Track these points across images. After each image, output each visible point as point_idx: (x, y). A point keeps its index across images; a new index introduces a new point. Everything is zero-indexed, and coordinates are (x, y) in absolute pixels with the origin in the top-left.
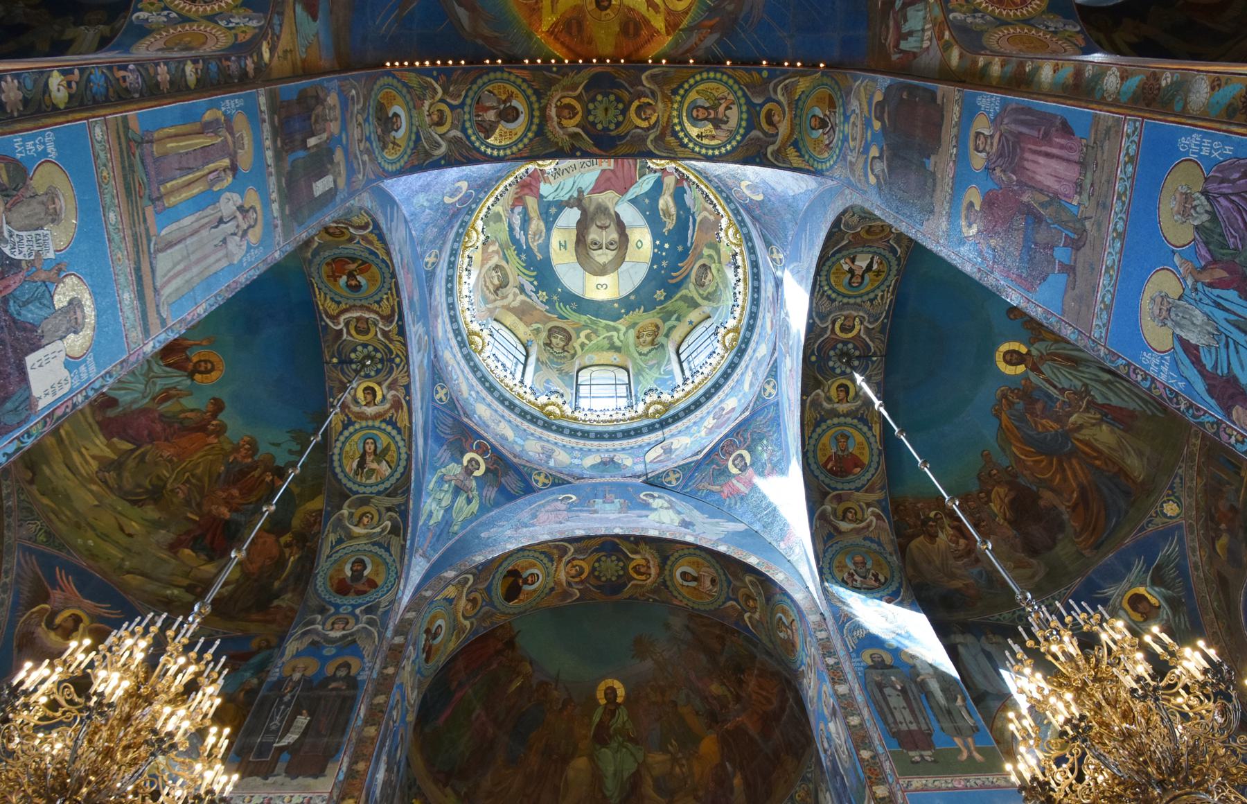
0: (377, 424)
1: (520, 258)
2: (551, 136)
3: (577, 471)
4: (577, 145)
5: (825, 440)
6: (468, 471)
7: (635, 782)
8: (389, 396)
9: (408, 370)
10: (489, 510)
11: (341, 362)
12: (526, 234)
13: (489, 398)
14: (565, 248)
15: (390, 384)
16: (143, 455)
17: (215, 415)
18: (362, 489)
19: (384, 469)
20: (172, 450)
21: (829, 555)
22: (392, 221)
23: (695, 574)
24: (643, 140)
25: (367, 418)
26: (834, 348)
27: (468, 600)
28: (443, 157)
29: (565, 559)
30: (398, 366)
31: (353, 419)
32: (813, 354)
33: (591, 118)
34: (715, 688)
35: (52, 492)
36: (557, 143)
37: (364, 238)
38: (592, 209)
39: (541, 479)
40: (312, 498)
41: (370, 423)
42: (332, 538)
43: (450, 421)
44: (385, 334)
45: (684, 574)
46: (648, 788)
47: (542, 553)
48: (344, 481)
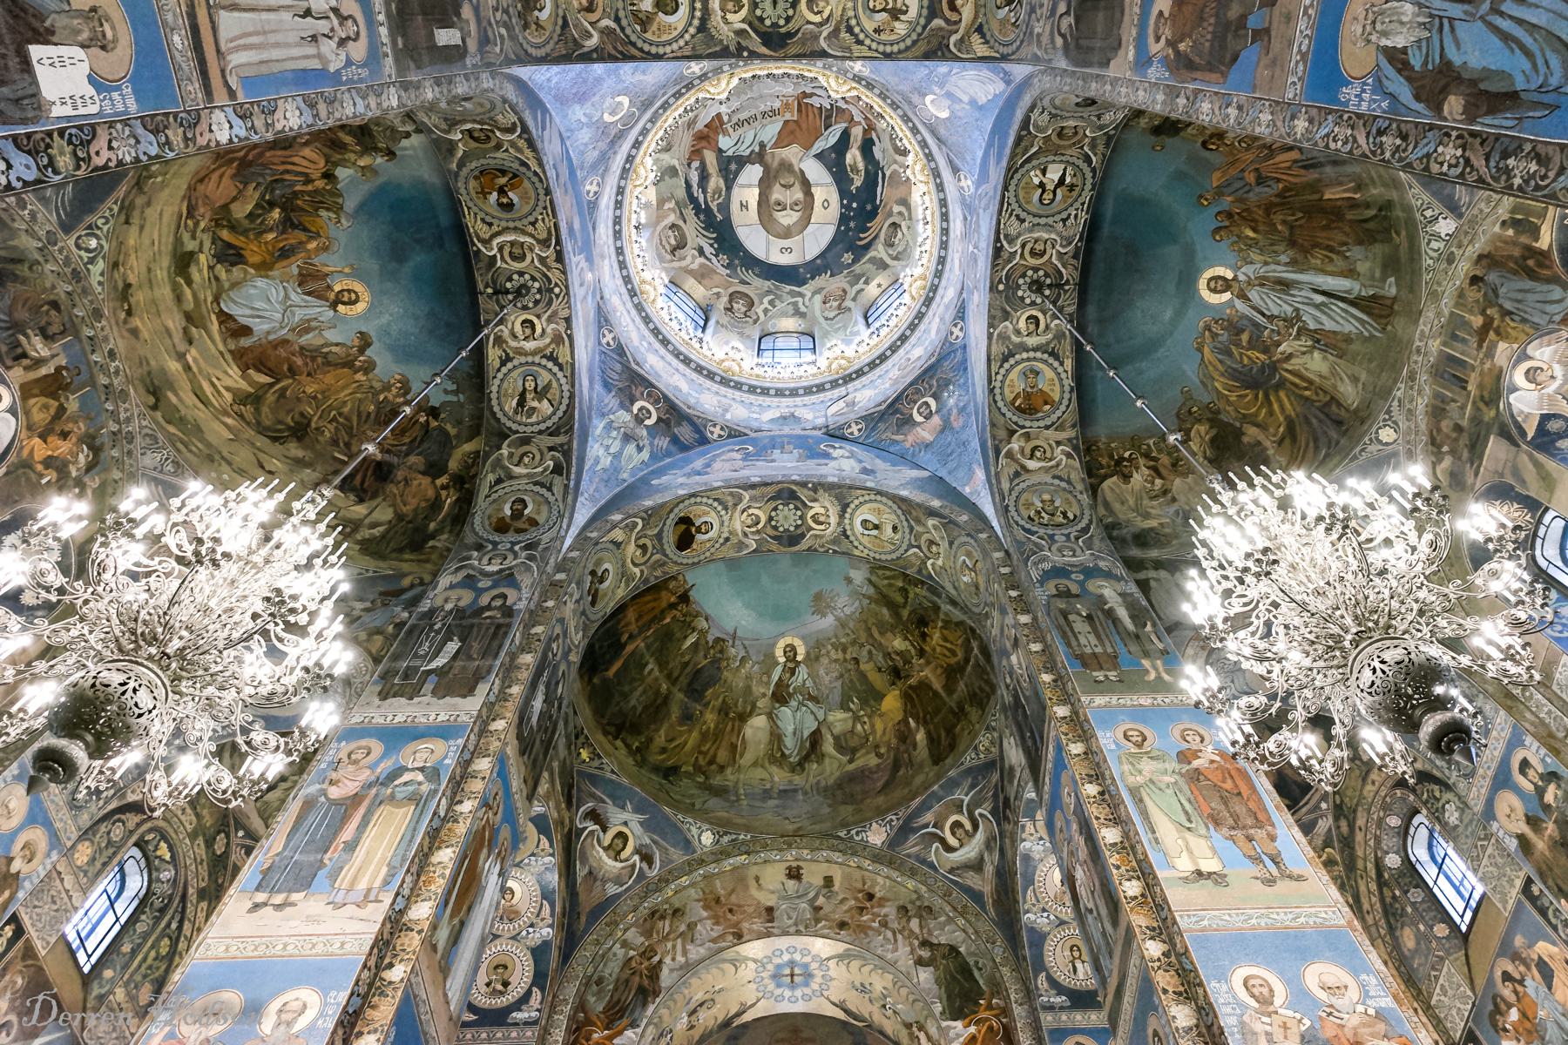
3: (755, 425)
5: (1014, 375)
6: (639, 420)
7: (816, 738)
10: (661, 459)
11: (496, 292)
13: (663, 351)
16: (284, 389)
17: (362, 351)
18: (522, 428)
19: (546, 409)
20: (316, 386)
21: (1014, 494)
22: (544, 129)
25: (526, 354)
26: (1024, 275)
28: (596, 50)
30: (557, 296)
32: (1000, 281)
34: (898, 644)
35: (181, 422)
37: (513, 144)
39: (717, 430)
40: (470, 439)
41: (530, 359)
42: (491, 477)
43: (618, 367)
44: (542, 260)
45: (864, 522)
46: (828, 746)
48: (504, 420)
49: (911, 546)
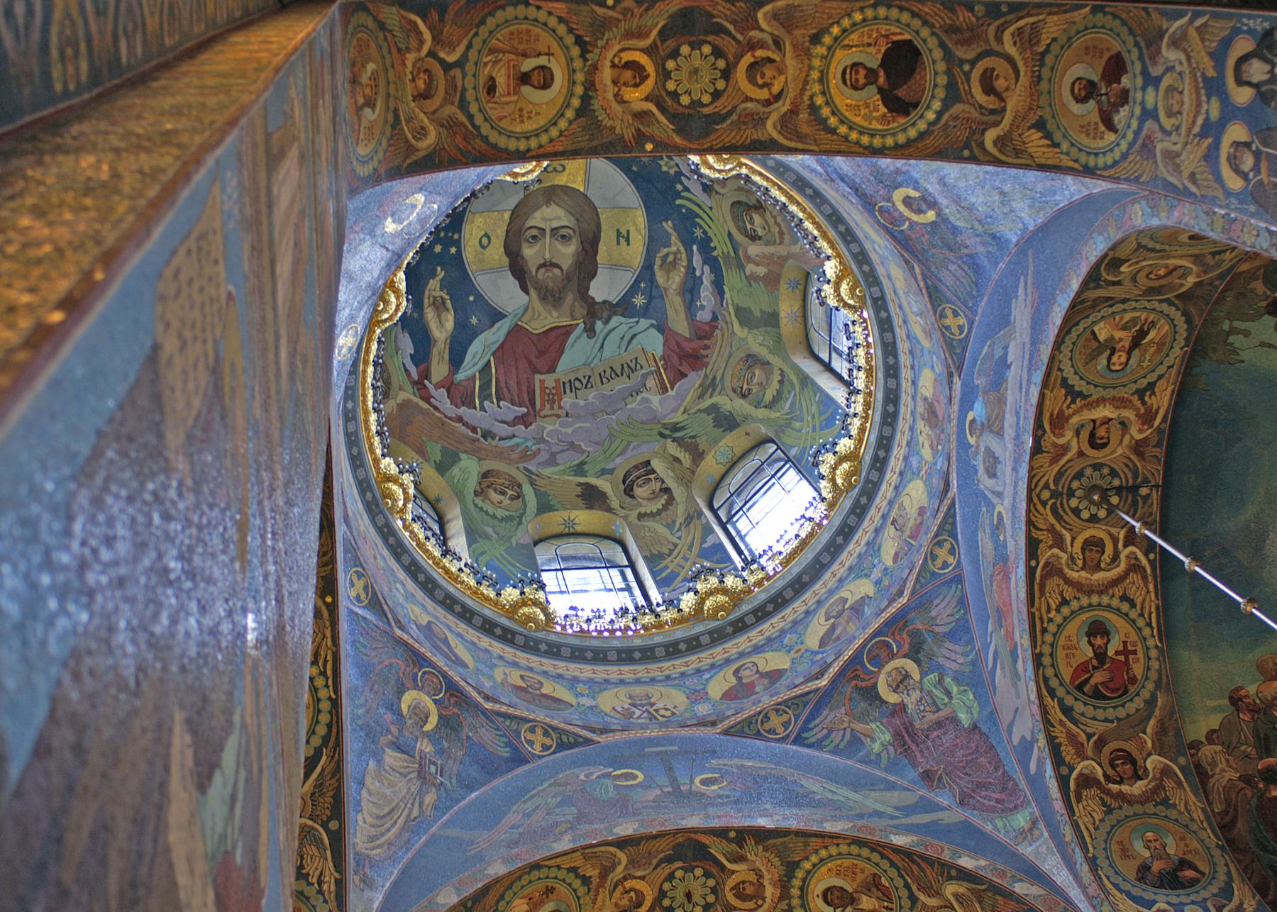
0: (1097, 393)
1: (705, 232)
2: (776, 861)
4: (734, 847)
8: (1069, 434)
9: (1030, 479)
11: (1135, 488)
12: (690, 269)
14: (619, 233)
15: (1064, 455)
23: (526, 89)
24: (632, 862)
27: (1002, 100)
29: (784, 106)
30: (1046, 486)
31: (1136, 397)
33: (711, 882)
36: (765, 850)
38: (569, 298)
42: (1227, 256)
44: (1059, 542)
45: (546, 85)
47: (833, 131)
49: (459, 64)
